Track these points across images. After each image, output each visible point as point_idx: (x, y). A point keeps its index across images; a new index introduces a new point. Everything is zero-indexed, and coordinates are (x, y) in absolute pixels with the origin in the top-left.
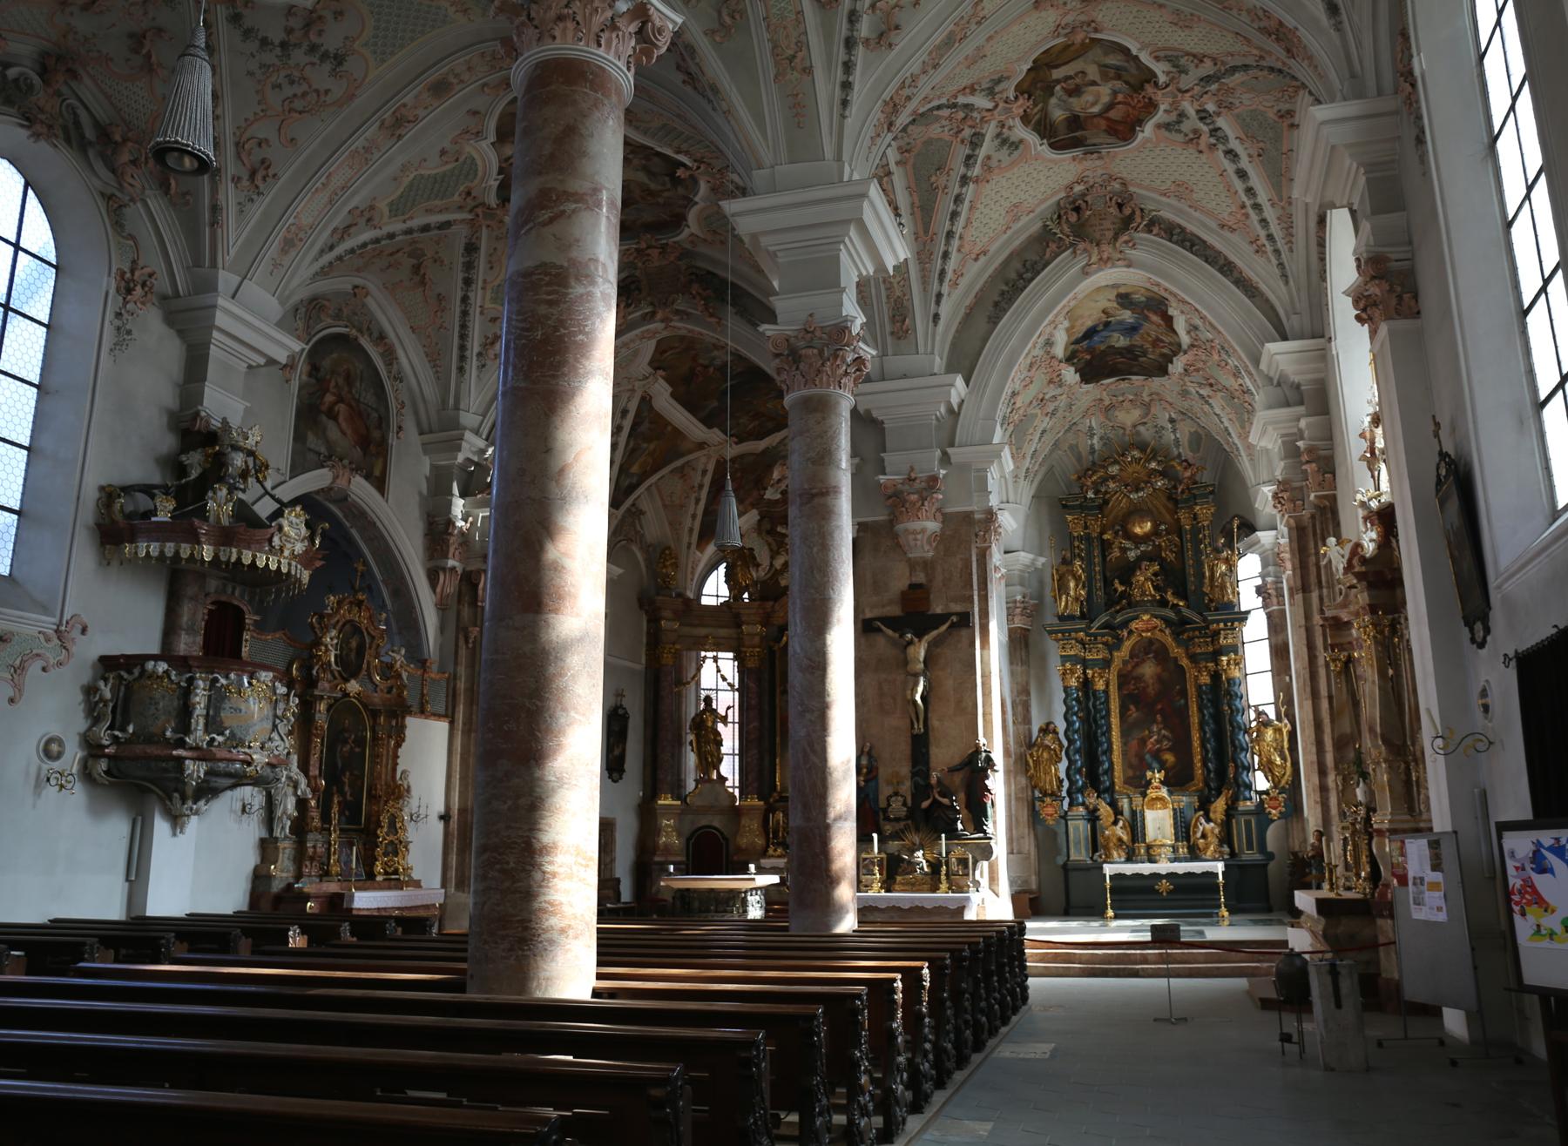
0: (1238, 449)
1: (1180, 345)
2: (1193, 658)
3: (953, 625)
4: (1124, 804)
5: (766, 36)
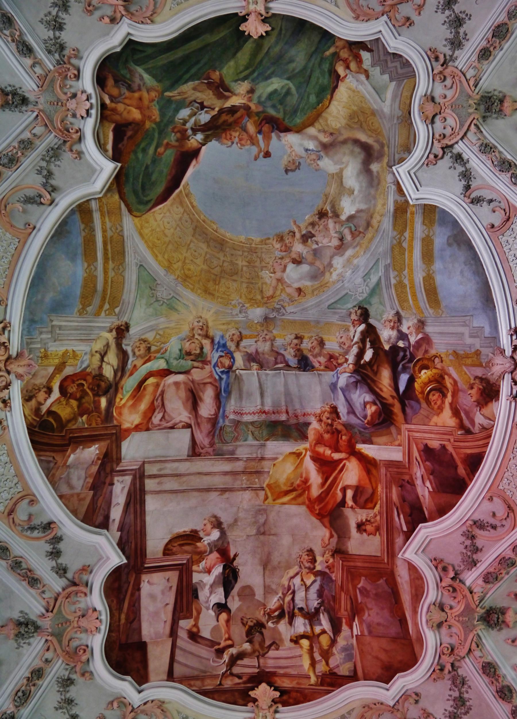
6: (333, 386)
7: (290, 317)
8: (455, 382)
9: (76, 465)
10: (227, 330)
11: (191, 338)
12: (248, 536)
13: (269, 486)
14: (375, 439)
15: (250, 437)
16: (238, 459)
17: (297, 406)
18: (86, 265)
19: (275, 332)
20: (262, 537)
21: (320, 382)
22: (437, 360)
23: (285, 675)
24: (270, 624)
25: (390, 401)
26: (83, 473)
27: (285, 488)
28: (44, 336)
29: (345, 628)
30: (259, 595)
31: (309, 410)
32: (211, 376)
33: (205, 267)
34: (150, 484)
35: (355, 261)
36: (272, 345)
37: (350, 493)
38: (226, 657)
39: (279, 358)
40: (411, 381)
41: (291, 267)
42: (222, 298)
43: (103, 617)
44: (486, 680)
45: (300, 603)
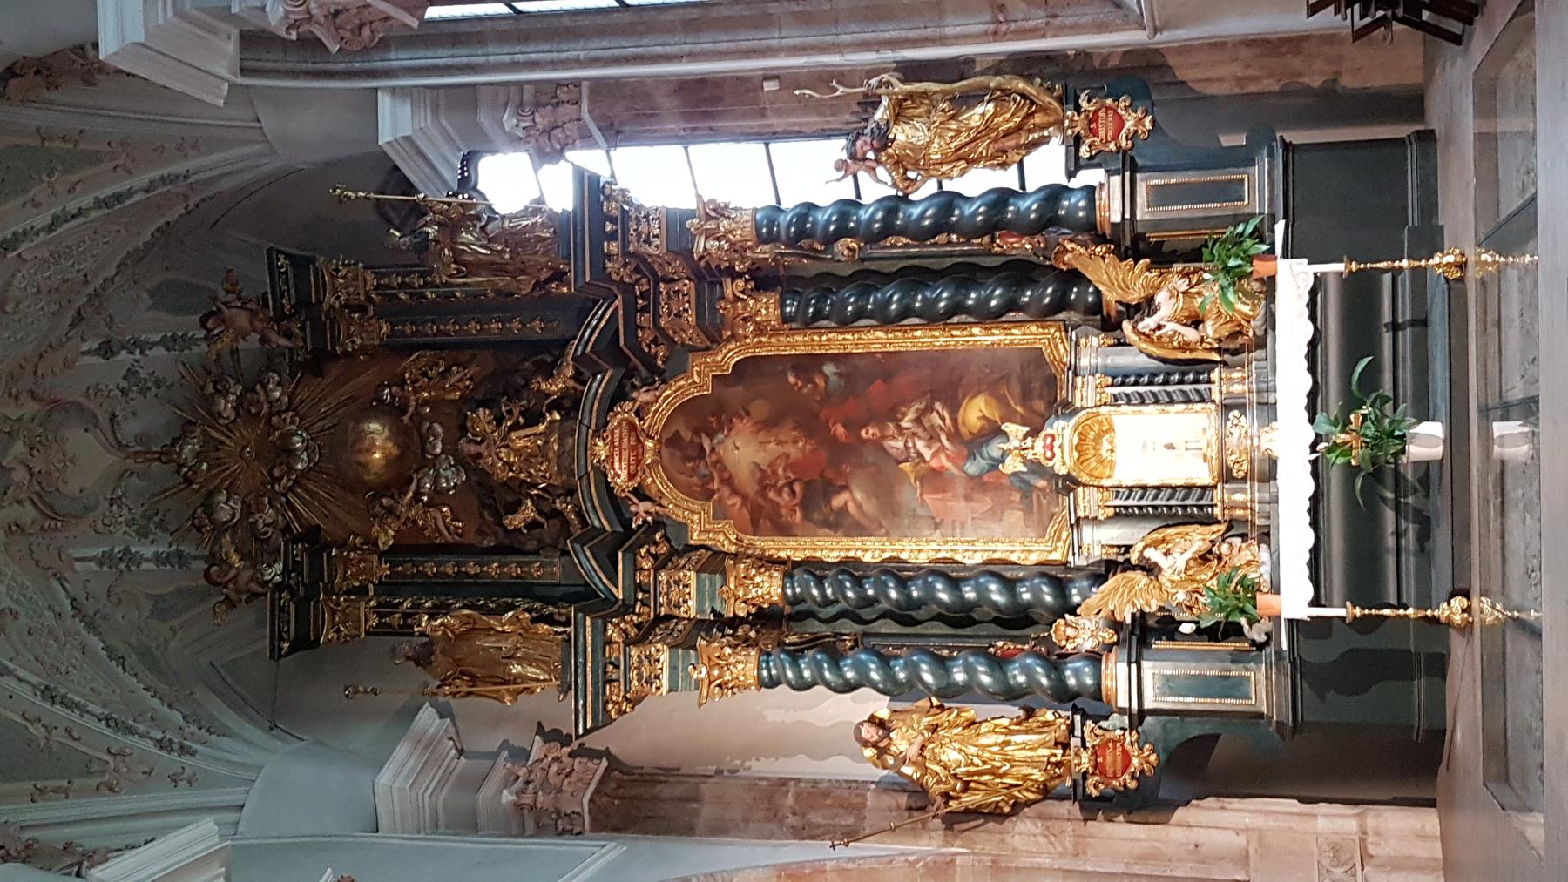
2: (714, 335)
4: (1099, 540)
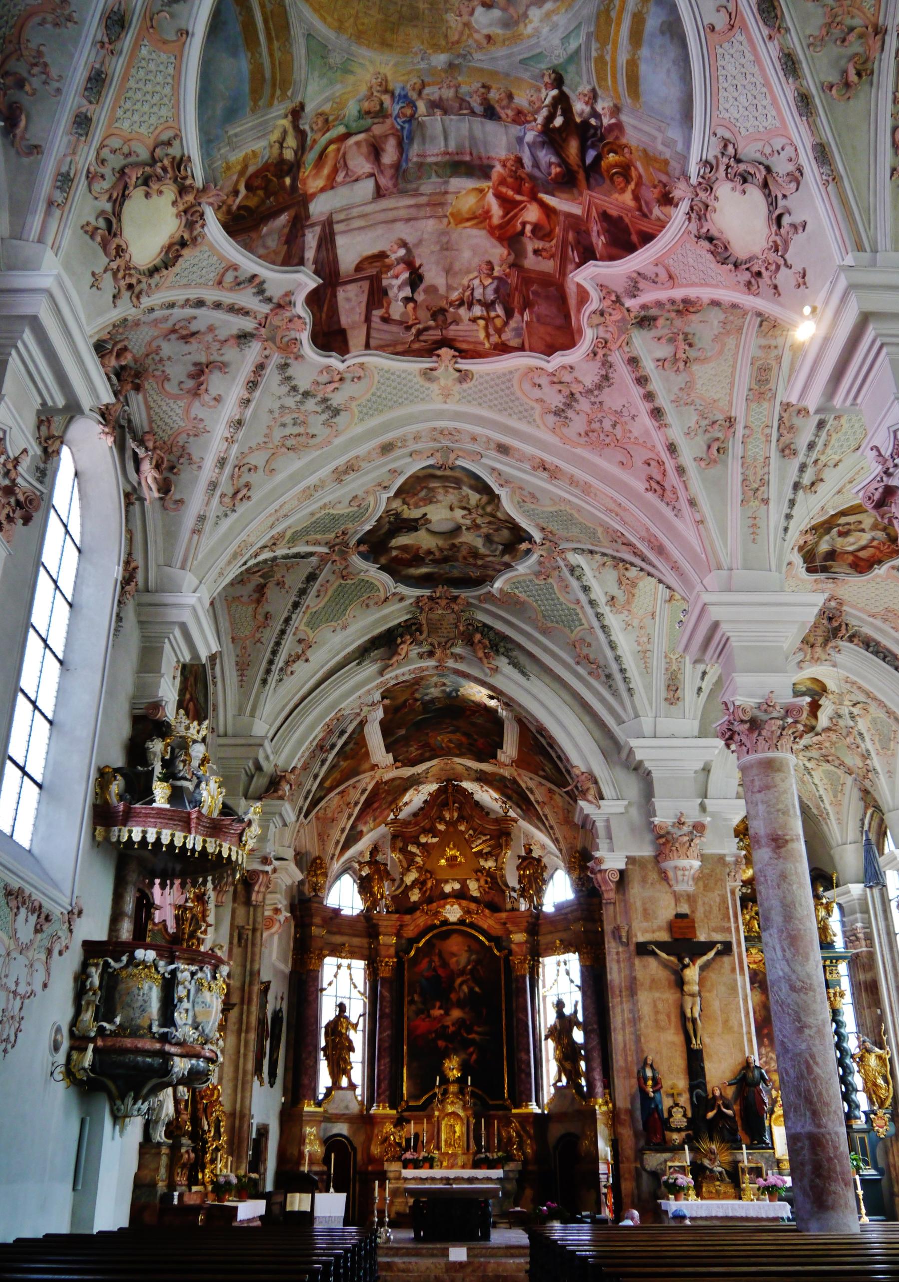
0: (827, 814)
1: (812, 728)
3: (718, 953)
5: (740, 470)
6: (520, 140)
7: (478, 65)
8: (640, 177)
9: (268, 234)
10: (407, 82)
11: (370, 97)
12: (432, 252)
13: (452, 214)
14: (557, 194)
15: (434, 175)
16: (422, 195)
17: (482, 151)
18: (249, 55)
19: (460, 79)
20: (445, 253)
21: (507, 134)
22: (626, 150)
23: (463, 341)
24: (452, 310)
25: (576, 168)
26: (276, 237)
27: (467, 216)
28: (222, 151)
29: (517, 315)
30: (442, 290)
31: (493, 154)
32: (393, 127)
33: (380, 17)
34: (337, 228)
35: (555, 18)
36: (457, 92)
37: (529, 228)
38: (413, 331)
39: (464, 105)
40: (598, 159)
41: (480, 10)
42: (401, 47)
43: (307, 321)
44: (630, 369)
45: (478, 294)
